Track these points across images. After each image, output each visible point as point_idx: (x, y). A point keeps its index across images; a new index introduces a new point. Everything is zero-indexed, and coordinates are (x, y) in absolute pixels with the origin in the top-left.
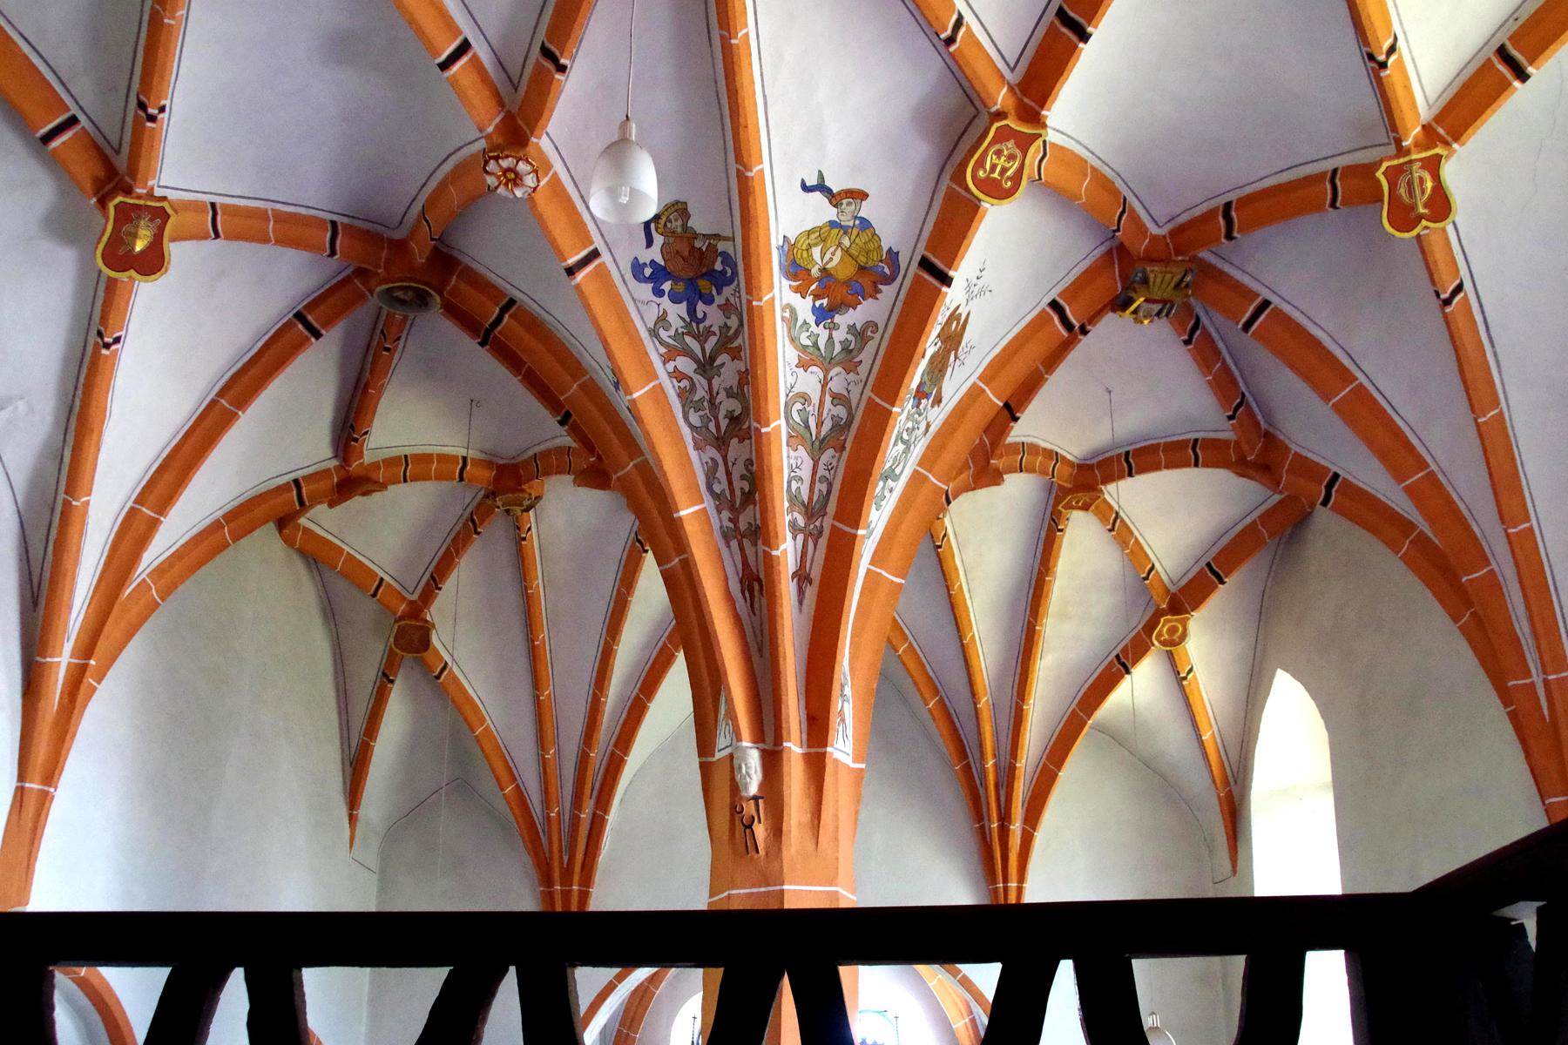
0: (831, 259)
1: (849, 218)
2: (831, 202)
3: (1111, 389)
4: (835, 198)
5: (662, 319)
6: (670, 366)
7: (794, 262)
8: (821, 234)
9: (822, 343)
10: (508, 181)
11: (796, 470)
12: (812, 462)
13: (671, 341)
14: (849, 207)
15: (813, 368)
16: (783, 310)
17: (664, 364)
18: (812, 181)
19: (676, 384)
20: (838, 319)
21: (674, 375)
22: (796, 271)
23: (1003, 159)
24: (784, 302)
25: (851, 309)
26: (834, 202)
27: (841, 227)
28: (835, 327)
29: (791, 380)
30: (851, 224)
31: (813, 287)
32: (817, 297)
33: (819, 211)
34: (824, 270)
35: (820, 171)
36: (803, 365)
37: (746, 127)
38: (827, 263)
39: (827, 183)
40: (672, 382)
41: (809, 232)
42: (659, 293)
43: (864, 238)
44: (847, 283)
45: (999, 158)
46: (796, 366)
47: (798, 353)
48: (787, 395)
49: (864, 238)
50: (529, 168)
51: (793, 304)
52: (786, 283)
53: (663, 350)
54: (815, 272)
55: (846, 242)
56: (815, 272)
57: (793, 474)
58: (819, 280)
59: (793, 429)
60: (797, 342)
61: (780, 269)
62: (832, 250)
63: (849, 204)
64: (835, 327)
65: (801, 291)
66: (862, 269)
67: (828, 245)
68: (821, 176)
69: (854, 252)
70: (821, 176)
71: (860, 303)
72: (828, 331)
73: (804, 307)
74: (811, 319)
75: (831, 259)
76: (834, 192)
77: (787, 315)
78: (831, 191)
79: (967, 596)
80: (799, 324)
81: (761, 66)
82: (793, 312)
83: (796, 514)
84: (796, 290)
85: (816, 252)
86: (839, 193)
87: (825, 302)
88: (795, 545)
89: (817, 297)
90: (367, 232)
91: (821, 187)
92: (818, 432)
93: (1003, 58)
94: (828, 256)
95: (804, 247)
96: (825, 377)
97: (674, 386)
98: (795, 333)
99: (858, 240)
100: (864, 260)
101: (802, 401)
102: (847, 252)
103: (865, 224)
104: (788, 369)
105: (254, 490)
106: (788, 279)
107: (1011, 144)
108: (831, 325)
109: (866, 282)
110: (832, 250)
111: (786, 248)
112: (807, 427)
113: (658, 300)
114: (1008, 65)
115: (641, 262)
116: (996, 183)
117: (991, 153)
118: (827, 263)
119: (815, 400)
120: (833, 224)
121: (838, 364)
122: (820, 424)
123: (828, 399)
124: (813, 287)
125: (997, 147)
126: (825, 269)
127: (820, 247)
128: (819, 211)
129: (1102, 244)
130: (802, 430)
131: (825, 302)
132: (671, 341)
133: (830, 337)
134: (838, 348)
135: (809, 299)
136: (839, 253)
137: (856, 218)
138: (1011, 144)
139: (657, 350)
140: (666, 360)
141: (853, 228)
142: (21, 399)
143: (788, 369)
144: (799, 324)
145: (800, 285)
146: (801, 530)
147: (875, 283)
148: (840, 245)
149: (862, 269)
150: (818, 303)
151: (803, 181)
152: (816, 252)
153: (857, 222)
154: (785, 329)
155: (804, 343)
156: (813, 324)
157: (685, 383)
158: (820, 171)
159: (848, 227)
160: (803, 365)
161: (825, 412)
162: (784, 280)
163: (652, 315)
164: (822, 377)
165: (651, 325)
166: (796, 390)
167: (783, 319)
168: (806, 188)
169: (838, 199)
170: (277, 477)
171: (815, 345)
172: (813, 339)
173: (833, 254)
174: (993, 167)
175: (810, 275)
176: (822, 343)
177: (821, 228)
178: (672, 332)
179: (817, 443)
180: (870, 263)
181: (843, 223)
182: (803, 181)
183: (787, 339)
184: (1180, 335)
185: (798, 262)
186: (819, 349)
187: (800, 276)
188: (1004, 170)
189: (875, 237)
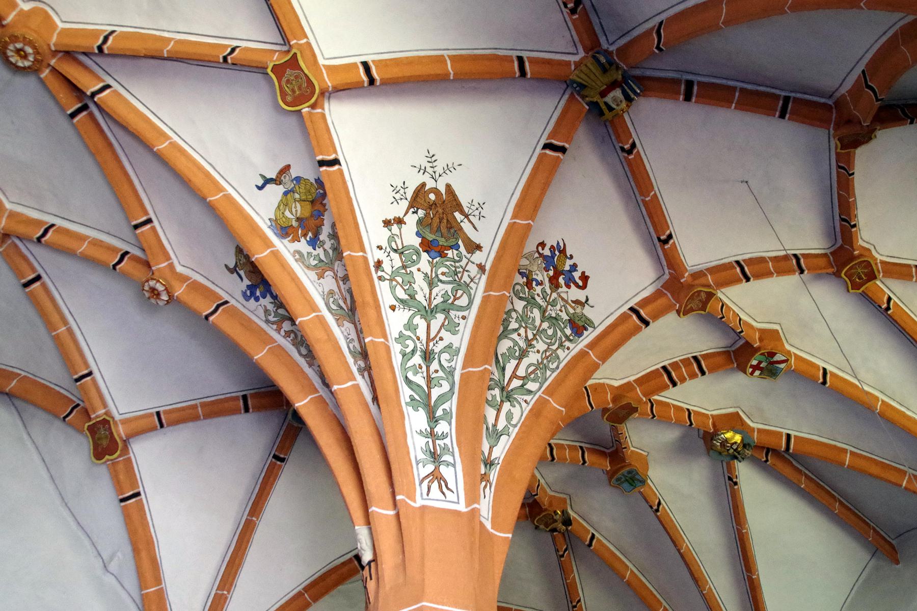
0: (296, 211)
1: (289, 183)
2: (277, 184)
3: (745, 180)
4: (276, 181)
5: (266, 311)
6: (283, 333)
7: (282, 228)
8: (284, 203)
9: (323, 257)
10: (542, 362)
11: (349, 336)
12: (353, 325)
13: (275, 319)
14: (286, 179)
15: (327, 273)
16: (294, 256)
17: (279, 333)
18: (260, 182)
19: (289, 339)
20: (322, 237)
21: (286, 335)
22: (284, 231)
23: (294, 82)
24: (292, 251)
25: (323, 227)
26: (278, 183)
27: (290, 191)
28: (323, 243)
29: (320, 289)
30: (293, 185)
31: (300, 232)
32: (305, 235)
33: (275, 192)
34: (298, 219)
35: (260, 175)
36: (321, 276)
37: (190, 181)
38: (296, 214)
39: (268, 177)
40: (287, 340)
41: (279, 207)
42: (257, 299)
43: (302, 186)
44: (312, 216)
45: (291, 83)
46: (319, 280)
47: (315, 272)
48: (324, 299)
49: (302, 186)
50: (155, 282)
51: (297, 249)
52: (286, 241)
53: (275, 327)
54: (295, 224)
55: (297, 196)
56: (295, 224)
57: (348, 340)
58: (300, 226)
59: (336, 315)
60: (311, 267)
61: (277, 236)
62: (293, 206)
63: (285, 177)
64: (323, 243)
65: (296, 239)
66: (312, 202)
67: (290, 205)
68: (263, 176)
69: (304, 197)
70: (263, 176)
71: (324, 219)
72: (321, 248)
73: (303, 246)
74: (310, 249)
75: (296, 211)
76: (274, 177)
77: (297, 256)
78: (272, 179)
79: (903, 409)
80: (306, 256)
81: (197, 153)
82: (299, 252)
83: (359, 362)
84: (293, 241)
85: (287, 213)
86: (277, 177)
87: (310, 234)
88: (365, 380)
89: (305, 235)
90: (267, 392)
91: (268, 181)
92: (347, 306)
93: (277, 44)
94: (294, 210)
95: (281, 216)
96: (334, 273)
97: (289, 342)
98: (307, 263)
99: (301, 190)
100: (310, 197)
101: (331, 295)
102: (301, 200)
103: (298, 179)
104: (315, 284)
105: (325, 569)
106: (285, 238)
107: (288, 71)
108: (321, 244)
109: (318, 206)
110: (293, 206)
111: (274, 224)
112: (341, 308)
113: (259, 303)
114: (281, 44)
115: (244, 290)
116: (301, 95)
117: (285, 86)
118: (296, 214)
119: (336, 290)
120: (286, 194)
121: (335, 261)
122: (345, 303)
123: (341, 283)
124: (300, 232)
125: (284, 80)
126: (297, 218)
127: (287, 210)
128: (275, 192)
129: (564, 93)
130: (340, 312)
131: (310, 234)
132: (275, 319)
133: (325, 250)
134: (331, 252)
135: (303, 240)
136: (298, 205)
137: (292, 181)
138: (288, 71)
139: (272, 328)
140: (278, 330)
141: (295, 187)
142: (118, 551)
143: (315, 284)
144: (306, 256)
145: (293, 236)
146: (365, 370)
147: (321, 203)
148: (295, 200)
149: (312, 202)
150: (308, 239)
151: (257, 186)
152: (287, 213)
153: (295, 182)
154: (301, 264)
155: (313, 264)
156: (312, 251)
157: (292, 335)
158: (260, 175)
159: (293, 188)
160: (321, 276)
161: (343, 291)
162: (283, 241)
163: (261, 312)
164: (332, 274)
165: (264, 319)
166: (326, 293)
167: (296, 260)
168: (260, 188)
169: (278, 179)
170: (340, 557)
171: (321, 261)
172: (317, 258)
173: (296, 207)
174: (293, 91)
175: (294, 227)
176: (323, 257)
177: (281, 200)
178: (273, 314)
179: (350, 313)
180: (314, 195)
181: (289, 189)
182: (257, 186)
183: (306, 270)
184: (678, 99)
185: (283, 226)
186: (323, 261)
187: (290, 232)
188: (300, 88)
189: (306, 181)
